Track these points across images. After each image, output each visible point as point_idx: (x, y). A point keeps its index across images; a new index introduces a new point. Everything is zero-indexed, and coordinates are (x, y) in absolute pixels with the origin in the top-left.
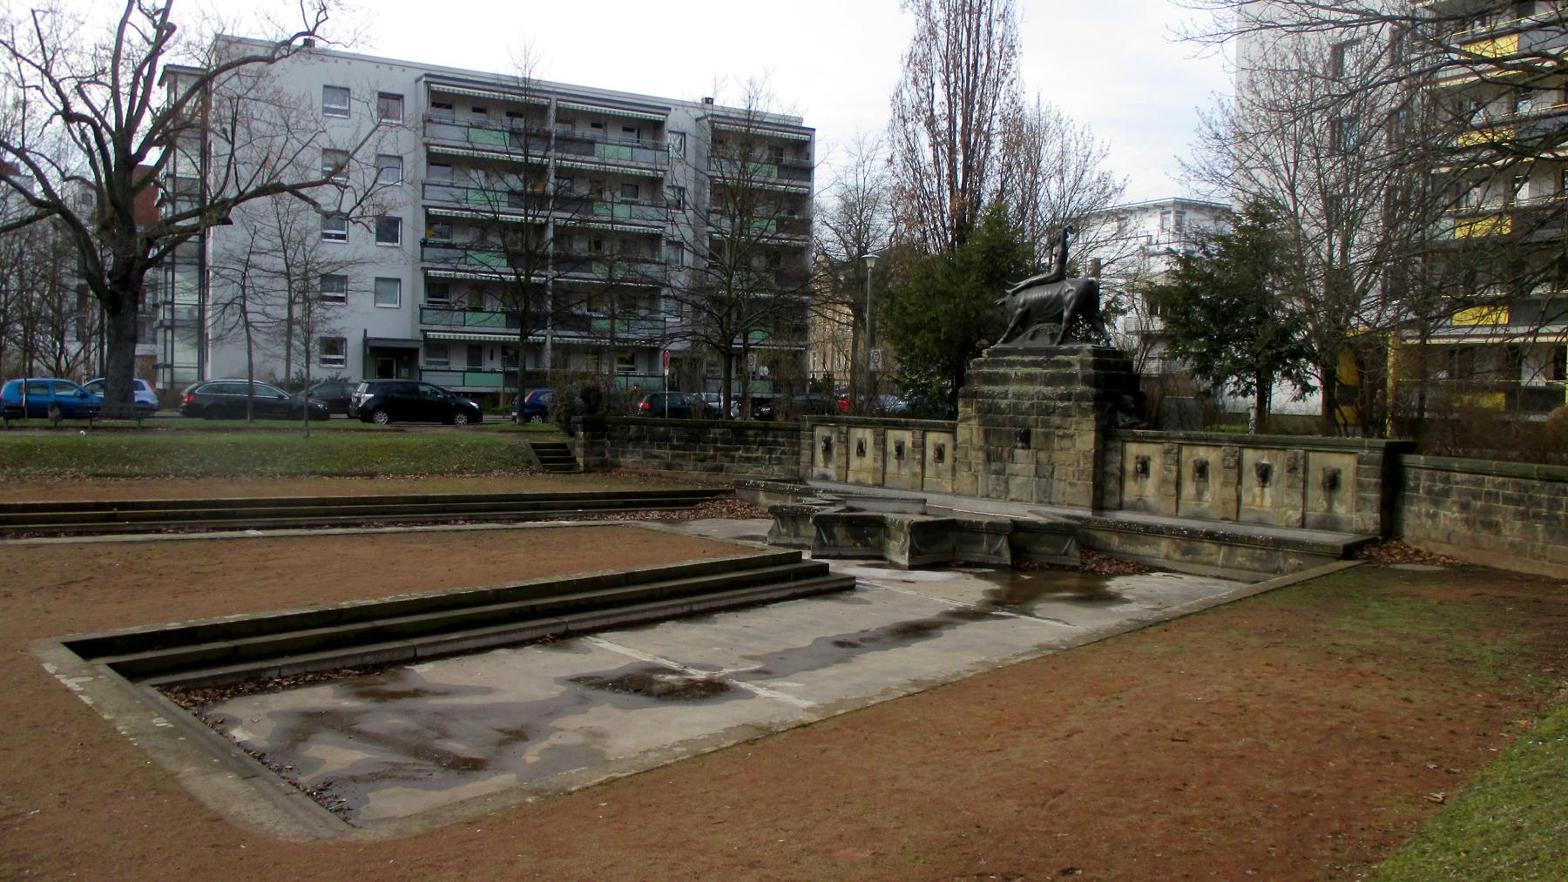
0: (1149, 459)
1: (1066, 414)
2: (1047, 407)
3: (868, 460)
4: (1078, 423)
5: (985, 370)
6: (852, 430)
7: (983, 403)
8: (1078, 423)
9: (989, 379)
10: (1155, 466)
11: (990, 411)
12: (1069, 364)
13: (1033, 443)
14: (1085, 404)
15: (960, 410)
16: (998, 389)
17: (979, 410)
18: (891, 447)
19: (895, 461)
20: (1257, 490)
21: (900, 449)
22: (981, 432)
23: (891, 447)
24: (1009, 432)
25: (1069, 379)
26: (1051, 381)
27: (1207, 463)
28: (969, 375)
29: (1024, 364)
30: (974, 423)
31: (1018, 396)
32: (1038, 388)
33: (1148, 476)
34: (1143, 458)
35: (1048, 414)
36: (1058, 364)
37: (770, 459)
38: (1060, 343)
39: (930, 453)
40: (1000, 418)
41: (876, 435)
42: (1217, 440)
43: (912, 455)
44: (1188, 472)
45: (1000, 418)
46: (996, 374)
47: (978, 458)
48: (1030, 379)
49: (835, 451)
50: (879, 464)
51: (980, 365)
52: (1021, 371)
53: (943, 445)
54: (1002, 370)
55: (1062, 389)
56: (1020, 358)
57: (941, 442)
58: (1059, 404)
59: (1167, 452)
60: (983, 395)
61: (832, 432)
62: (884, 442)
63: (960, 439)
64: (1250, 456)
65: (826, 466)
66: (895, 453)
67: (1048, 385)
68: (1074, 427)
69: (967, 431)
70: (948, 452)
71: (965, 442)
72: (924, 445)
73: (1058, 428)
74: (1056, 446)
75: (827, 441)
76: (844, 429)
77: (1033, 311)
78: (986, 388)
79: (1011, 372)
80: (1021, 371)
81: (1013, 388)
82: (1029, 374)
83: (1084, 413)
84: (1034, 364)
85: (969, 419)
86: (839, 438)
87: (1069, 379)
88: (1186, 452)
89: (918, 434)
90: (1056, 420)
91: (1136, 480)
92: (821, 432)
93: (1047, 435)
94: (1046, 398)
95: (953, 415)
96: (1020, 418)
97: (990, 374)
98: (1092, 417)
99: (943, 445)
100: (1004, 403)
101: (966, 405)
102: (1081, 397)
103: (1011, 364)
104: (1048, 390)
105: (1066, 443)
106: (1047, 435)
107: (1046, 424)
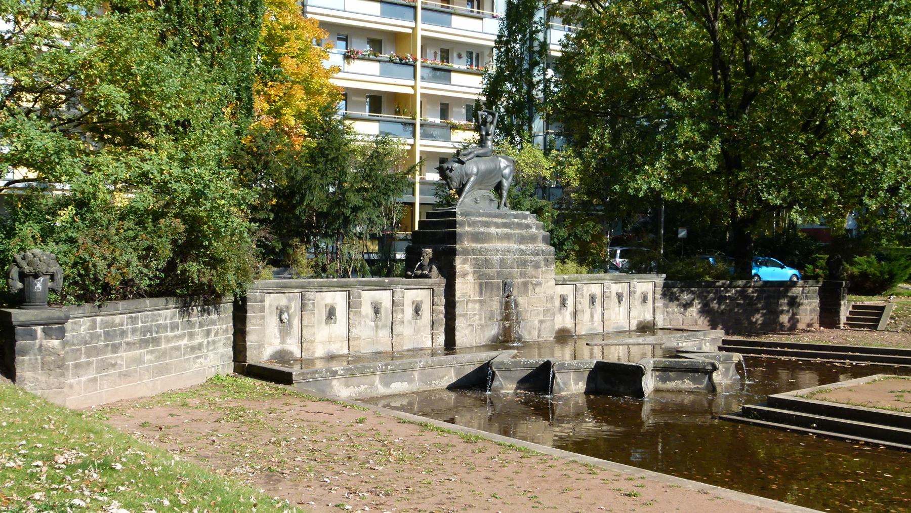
1: (537, 266)
3: (340, 326)
9: (476, 238)
10: (570, 302)
12: (528, 226)
16: (486, 245)
18: (367, 309)
20: (617, 309)
22: (477, 287)
23: (367, 309)
25: (533, 239)
26: (522, 240)
29: (497, 225)
30: (470, 277)
32: (514, 246)
36: (520, 226)
37: (208, 342)
39: (409, 311)
44: (586, 301)
46: (482, 233)
47: (474, 309)
48: (507, 237)
52: (500, 231)
53: (422, 302)
54: (482, 229)
57: (419, 299)
64: (615, 288)
65: (283, 341)
67: (521, 243)
78: (478, 246)
79: (493, 230)
81: (499, 245)
82: (506, 234)
84: (505, 225)
87: (533, 239)
90: (530, 270)
91: (560, 313)
92: (273, 300)
93: (525, 284)
94: (523, 252)
99: (422, 302)
100: (496, 258)
101: (465, 261)
103: (488, 225)
104: (523, 247)
106: (525, 284)
107: (523, 275)
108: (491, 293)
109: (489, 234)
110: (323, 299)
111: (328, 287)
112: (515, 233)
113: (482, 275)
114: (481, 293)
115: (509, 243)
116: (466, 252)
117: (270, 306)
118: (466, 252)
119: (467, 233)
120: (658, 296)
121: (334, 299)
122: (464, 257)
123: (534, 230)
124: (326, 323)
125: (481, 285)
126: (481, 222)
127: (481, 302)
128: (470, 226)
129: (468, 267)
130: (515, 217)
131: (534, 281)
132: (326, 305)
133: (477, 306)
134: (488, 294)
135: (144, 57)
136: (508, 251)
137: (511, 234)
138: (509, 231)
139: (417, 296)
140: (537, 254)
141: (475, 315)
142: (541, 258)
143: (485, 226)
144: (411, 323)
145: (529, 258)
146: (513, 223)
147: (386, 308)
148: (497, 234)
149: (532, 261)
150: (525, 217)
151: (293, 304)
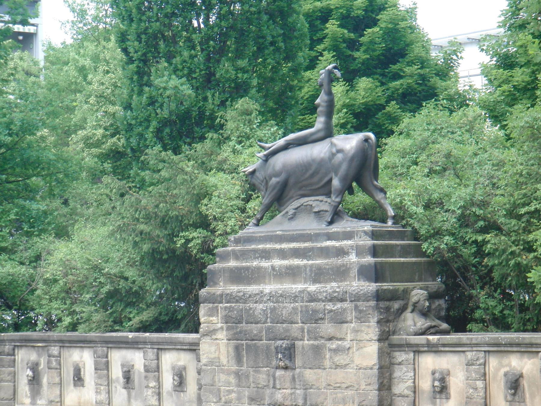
0: (449, 374)
2: (315, 311)
4: (356, 331)
5: (232, 263)
6: (66, 353)
7: (230, 309)
8: (356, 331)
11: (240, 322)
12: (341, 252)
13: (298, 362)
14: (363, 305)
15: (202, 320)
16: (253, 289)
17: (227, 320)
18: (117, 372)
19: (124, 392)
21: (128, 377)
22: (231, 350)
23: (117, 372)
24: (268, 347)
27: (521, 376)
28: (213, 272)
29: (283, 254)
31: (274, 297)
32: (299, 286)
33: (448, 398)
34: (441, 373)
35: (316, 321)
36: (325, 252)
38: (331, 223)
40: (254, 328)
41: (97, 356)
42: (531, 345)
43: (145, 383)
45: (254, 328)
46: (247, 269)
47: (229, 384)
49: (45, 381)
50: (103, 397)
51: (225, 257)
52: (278, 262)
53: (185, 368)
54: (255, 263)
55: (332, 286)
56: (278, 246)
57: (181, 363)
58: (330, 306)
59: (469, 364)
60: (230, 298)
61: (39, 356)
62: (107, 365)
63: (204, 360)
66: (122, 380)
67: (315, 281)
68: (349, 337)
69: (213, 349)
70: (191, 377)
71: (211, 363)
72: (158, 369)
73: (330, 339)
74: (327, 363)
75: (34, 368)
76: (55, 350)
77: (292, 181)
78: (234, 288)
80: (278, 262)
81: (268, 288)
83: (362, 317)
84: (296, 253)
85: (215, 331)
86: (49, 362)
88: (493, 362)
89: (151, 354)
94: (313, 298)
95: (195, 328)
96: (280, 327)
97: (239, 269)
98: (373, 322)
99: (185, 368)
101: (212, 312)
102: (356, 298)
103: (266, 255)
105: (340, 359)
106: (317, 351)
108: (255, 361)
109: (259, 269)
110: (70, 356)
111: (70, 342)
112: (305, 266)
113: (241, 332)
114: (239, 359)
115: (294, 282)
116: (213, 299)
117: (22, 360)
118: (213, 299)
119: (224, 269)
120: (82, 370)
121: (81, 357)
122: (211, 305)
123: (353, 258)
124: (75, 385)
125: (237, 348)
126: (255, 251)
127: (237, 374)
128: (237, 258)
129: (217, 321)
130: (330, 237)
131: (334, 345)
132: (73, 364)
133: (232, 379)
134: (251, 363)
135: (244, 70)
136: (281, 296)
137: (298, 267)
138: (305, 262)
139: (179, 360)
140: (342, 300)
141: (230, 392)
142: (346, 305)
143: (262, 257)
144: (172, 396)
145: (320, 306)
146: (312, 249)
147: (140, 372)
148: (273, 268)
149: (331, 311)
150: (349, 235)
151: (42, 360)
